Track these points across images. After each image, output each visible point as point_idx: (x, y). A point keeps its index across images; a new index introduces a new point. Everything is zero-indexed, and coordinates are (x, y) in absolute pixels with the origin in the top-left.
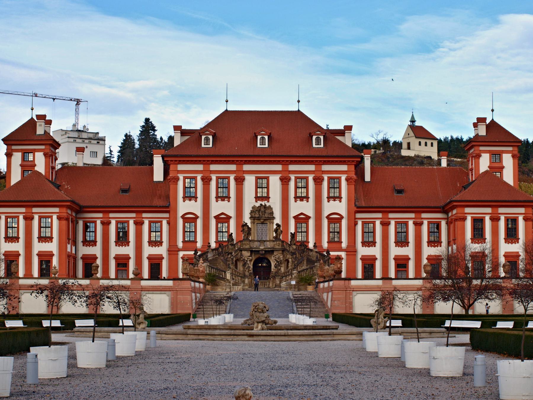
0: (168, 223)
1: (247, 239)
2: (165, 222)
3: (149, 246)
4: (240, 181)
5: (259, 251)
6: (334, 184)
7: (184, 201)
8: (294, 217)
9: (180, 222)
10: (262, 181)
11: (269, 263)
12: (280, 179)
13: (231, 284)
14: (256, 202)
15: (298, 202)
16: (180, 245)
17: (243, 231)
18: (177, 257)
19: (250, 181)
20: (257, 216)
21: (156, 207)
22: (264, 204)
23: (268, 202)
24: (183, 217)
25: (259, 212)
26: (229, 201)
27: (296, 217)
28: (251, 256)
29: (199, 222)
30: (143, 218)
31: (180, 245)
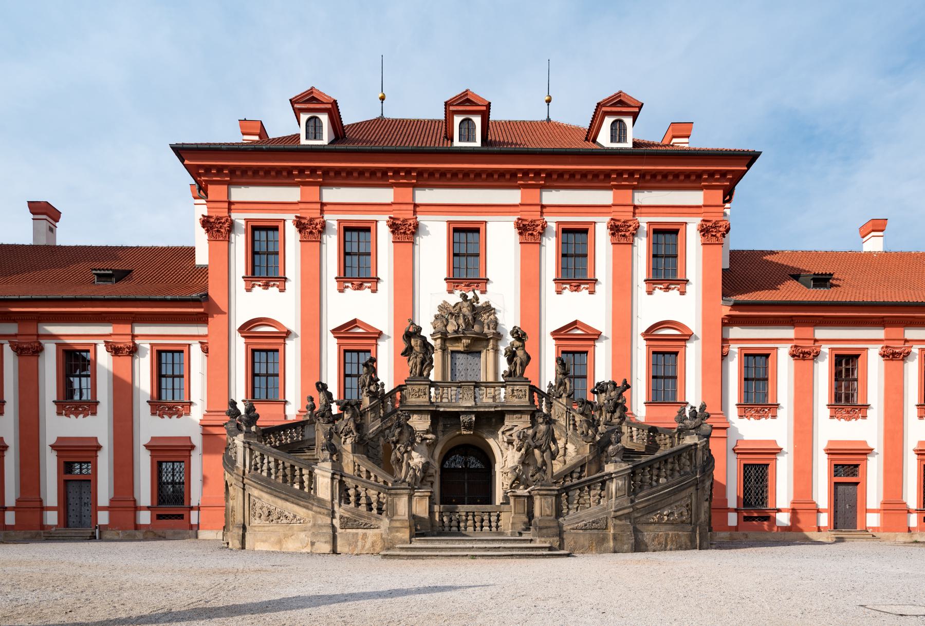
0: (205, 350)
1: (420, 375)
5: (457, 415)
6: (666, 239)
8: (555, 333)
9: (239, 346)
10: (466, 241)
11: (488, 459)
13: (337, 522)
14: (450, 292)
15: (567, 292)
17: (408, 352)
22: (470, 295)
23: (484, 292)
25: (457, 317)
26: (374, 291)
28: (433, 429)
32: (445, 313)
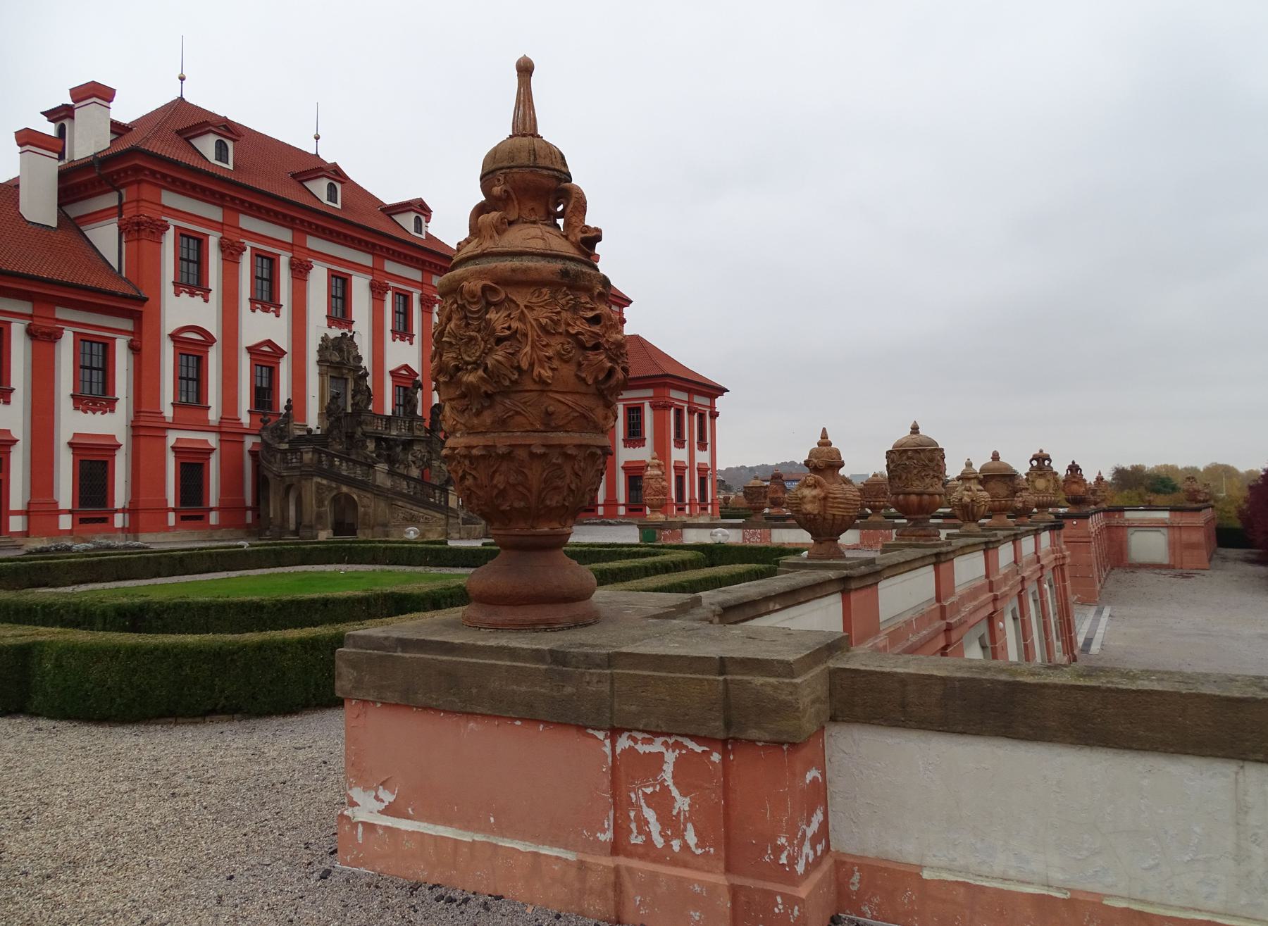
0: (135, 348)
2: (121, 345)
3: (76, 408)
4: (300, 271)
7: (177, 295)
12: (373, 286)
16: (168, 412)
18: (164, 444)
19: (318, 277)
20: (336, 358)
21: (113, 295)
24: (174, 337)
27: (393, 374)
29: (214, 358)
30: (58, 320)
31: (168, 412)
32: (327, 346)
